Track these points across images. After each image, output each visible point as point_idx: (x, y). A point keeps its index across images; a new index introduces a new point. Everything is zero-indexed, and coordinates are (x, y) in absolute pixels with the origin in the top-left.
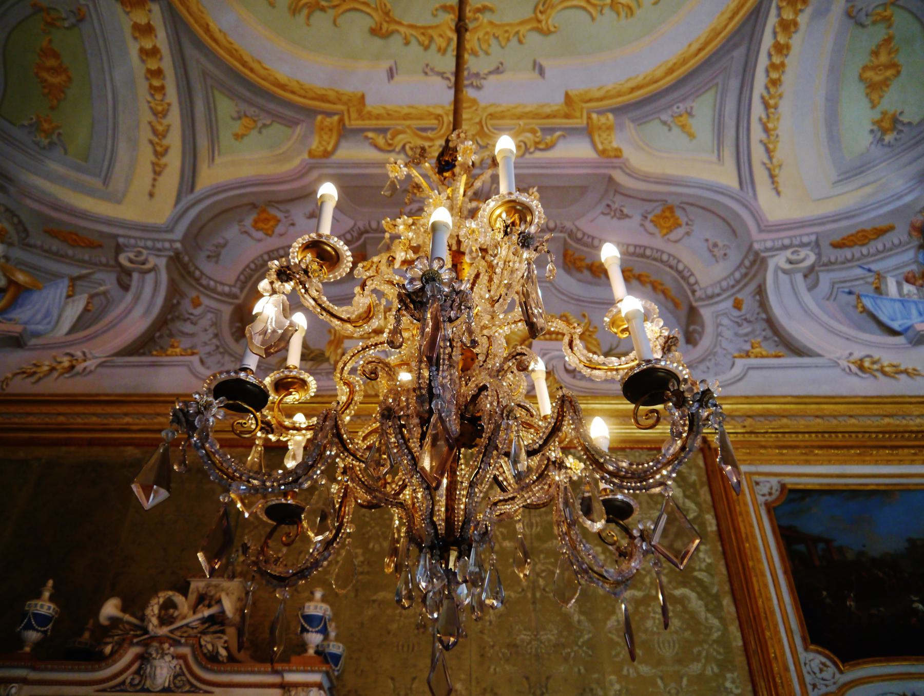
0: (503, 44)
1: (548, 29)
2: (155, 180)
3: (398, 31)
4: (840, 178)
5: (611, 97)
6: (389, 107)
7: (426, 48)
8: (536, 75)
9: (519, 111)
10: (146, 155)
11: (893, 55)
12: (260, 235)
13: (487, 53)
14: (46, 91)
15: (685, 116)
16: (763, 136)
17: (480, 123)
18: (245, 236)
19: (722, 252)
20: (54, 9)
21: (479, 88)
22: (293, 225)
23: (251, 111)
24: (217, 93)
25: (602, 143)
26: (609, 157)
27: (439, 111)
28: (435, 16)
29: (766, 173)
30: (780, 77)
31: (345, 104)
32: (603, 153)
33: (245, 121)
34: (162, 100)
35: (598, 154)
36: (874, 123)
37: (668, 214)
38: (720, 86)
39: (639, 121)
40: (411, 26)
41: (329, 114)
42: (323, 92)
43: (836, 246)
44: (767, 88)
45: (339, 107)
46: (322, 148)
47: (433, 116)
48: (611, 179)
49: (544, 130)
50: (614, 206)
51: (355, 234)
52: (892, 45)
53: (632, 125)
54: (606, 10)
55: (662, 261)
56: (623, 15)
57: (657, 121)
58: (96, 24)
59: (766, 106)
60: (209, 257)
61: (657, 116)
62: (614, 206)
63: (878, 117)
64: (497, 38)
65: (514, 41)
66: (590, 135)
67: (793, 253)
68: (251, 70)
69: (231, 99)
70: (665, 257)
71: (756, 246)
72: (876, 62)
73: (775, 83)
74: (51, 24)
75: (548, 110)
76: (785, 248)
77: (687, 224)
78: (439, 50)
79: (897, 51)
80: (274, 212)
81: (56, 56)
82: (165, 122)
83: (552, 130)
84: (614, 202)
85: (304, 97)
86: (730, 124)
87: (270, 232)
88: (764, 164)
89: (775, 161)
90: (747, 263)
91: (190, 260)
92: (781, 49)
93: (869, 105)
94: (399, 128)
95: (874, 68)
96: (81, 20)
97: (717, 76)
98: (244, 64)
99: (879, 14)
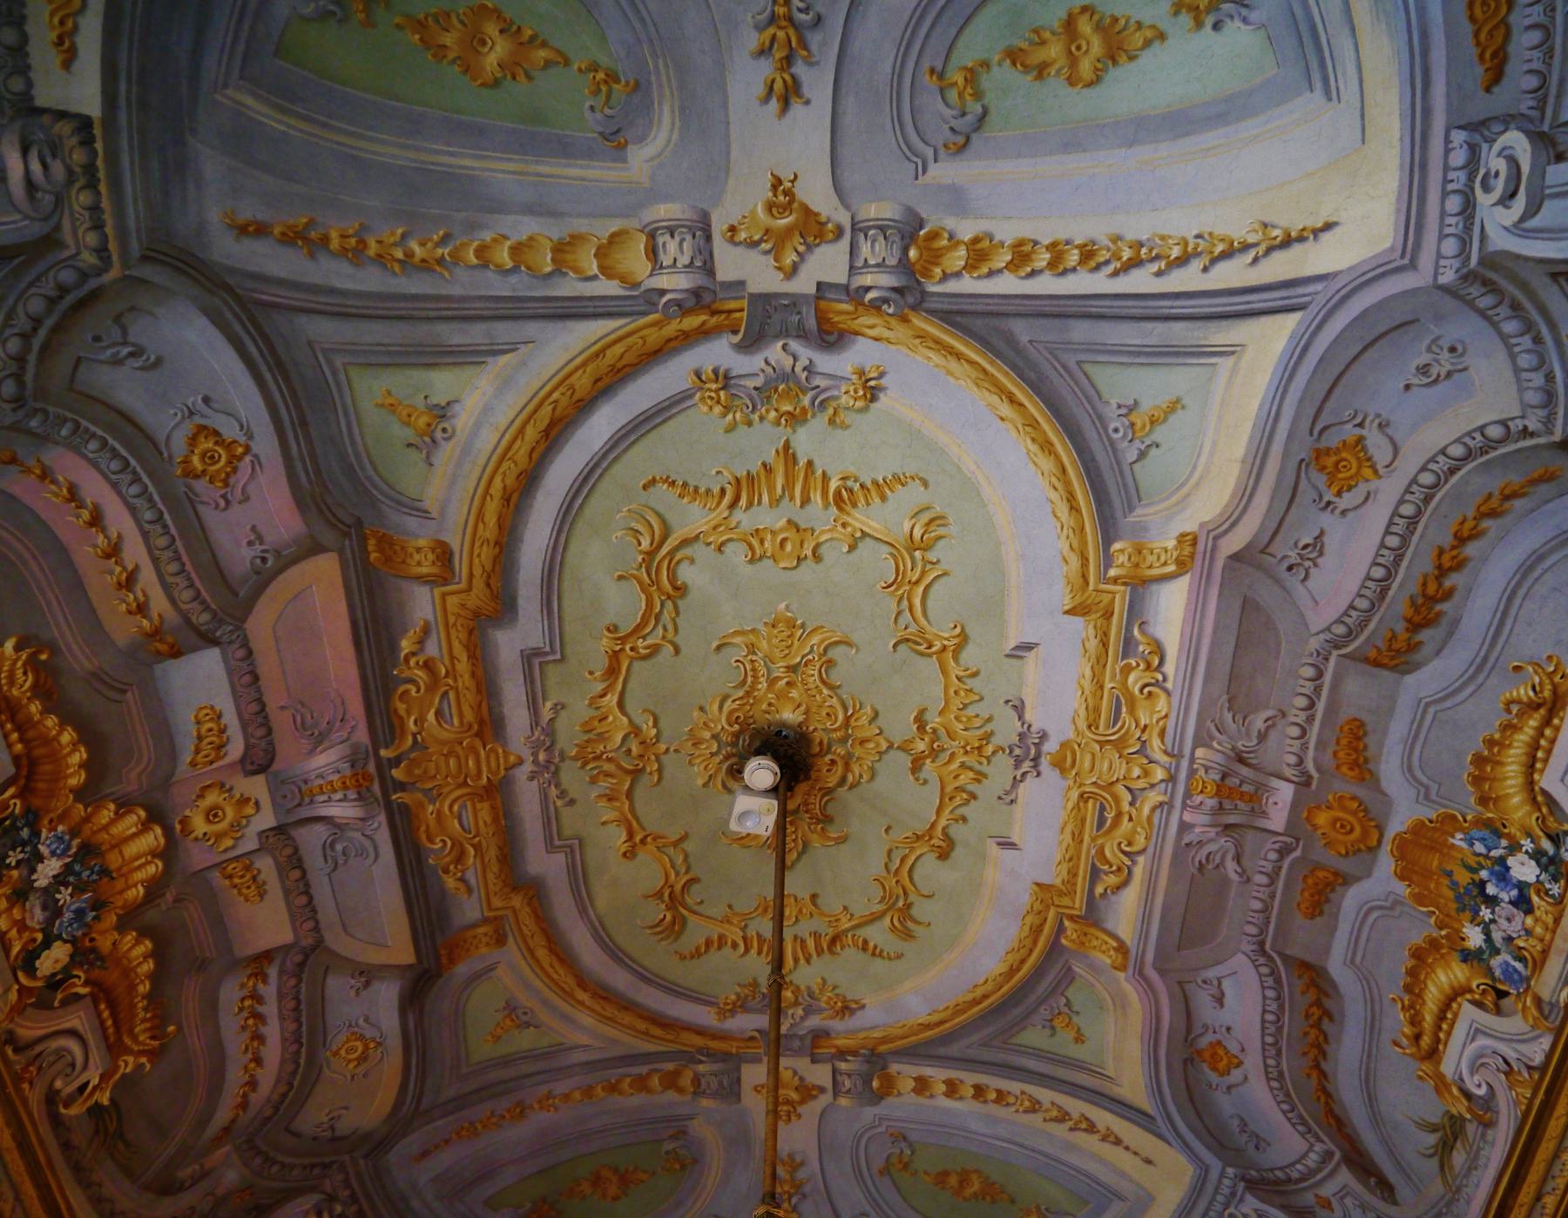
0: (977, 698)
1: (958, 636)
2: (1127, 1148)
3: (944, 829)
4: (1318, 85)
5: (1084, 543)
6: (1058, 857)
7: (973, 796)
8: (1031, 655)
9: (1087, 684)
10: (1090, 1142)
11: (1047, 35)
12: (1236, 1076)
13: (989, 720)
14: (988, 1198)
15: (1133, 418)
16: (1196, 265)
17: (1102, 744)
18: (1233, 1091)
19: (1446, 355)
20: (889, 1156)
21: (1044, 736)
22: (1228, 1029)
23: (1044, 1012)
24: (1014, 1040)
25: (1165, 564)
26: (1192, 556)
27: (1075, 794)
28: (925, 782)
29: (1279, 256)
30: (1077, 247)
31: (1048, 908)
32: (1183, 566)
33: (1056, 1022)
34: (1017, 1098)
35: (1187, 572)
36: (1199, 24)
37: (1330, 462)
38: (1082, 357)
39: (1134, 496)
40: (939, 812)
41: (1060, 930)
42: (1026, 928)
43: (1496, 75)
44: (1098, 268)
45: (1051, 913)
46: (1112, 953)
47: (1081, 804)
48: (1236, 557)
49: (1125, 655)
50: (1293, 557)
51: (1262, 960)
52: (1024, 45)
53: (1139, 511)
54: (932, 556)
55: (1436, 486)
56: (941, 531)
57: (1137, 467)
58: (913, 1126)
59: (1135, 263)
60: (1257, 1148)
61: (1127, 469)
62: (1293, 557)
63: (1186, 19)
64: (965, 706)
65: (971, 683)
66: (1146, 582)
67: (1487, 188)
68: (985, 997)
69: (1024, 1028)
70: (1427, 478)
71: (1447, 277)
72: (1062, 62)
73: (1087, 253)
74: (906, 1166)
75: (1093, 644)
76: (1468, 208)
77: (1361, 425)
78: (979, 781)
79: (1036, 31)
80: (1204, 1042)
81: (945, 1174)
82: (1047, 1105)
83: (1128, 645)
84: (1285, 557)
85: (1031, 951)
86: (1157, 333)
87: (1236, 1061)
88: (1256, 260)
89: (1251, 239)
90: (1485, 302)
91: (1258, 1171)
92: (1021, 255)
93: (1157, 44)
94: (1093, 852)
95: (1073, 62)
96: (905, 1139)
97: (1064, 366)
98: (976, 1002)
99: (961, 95)
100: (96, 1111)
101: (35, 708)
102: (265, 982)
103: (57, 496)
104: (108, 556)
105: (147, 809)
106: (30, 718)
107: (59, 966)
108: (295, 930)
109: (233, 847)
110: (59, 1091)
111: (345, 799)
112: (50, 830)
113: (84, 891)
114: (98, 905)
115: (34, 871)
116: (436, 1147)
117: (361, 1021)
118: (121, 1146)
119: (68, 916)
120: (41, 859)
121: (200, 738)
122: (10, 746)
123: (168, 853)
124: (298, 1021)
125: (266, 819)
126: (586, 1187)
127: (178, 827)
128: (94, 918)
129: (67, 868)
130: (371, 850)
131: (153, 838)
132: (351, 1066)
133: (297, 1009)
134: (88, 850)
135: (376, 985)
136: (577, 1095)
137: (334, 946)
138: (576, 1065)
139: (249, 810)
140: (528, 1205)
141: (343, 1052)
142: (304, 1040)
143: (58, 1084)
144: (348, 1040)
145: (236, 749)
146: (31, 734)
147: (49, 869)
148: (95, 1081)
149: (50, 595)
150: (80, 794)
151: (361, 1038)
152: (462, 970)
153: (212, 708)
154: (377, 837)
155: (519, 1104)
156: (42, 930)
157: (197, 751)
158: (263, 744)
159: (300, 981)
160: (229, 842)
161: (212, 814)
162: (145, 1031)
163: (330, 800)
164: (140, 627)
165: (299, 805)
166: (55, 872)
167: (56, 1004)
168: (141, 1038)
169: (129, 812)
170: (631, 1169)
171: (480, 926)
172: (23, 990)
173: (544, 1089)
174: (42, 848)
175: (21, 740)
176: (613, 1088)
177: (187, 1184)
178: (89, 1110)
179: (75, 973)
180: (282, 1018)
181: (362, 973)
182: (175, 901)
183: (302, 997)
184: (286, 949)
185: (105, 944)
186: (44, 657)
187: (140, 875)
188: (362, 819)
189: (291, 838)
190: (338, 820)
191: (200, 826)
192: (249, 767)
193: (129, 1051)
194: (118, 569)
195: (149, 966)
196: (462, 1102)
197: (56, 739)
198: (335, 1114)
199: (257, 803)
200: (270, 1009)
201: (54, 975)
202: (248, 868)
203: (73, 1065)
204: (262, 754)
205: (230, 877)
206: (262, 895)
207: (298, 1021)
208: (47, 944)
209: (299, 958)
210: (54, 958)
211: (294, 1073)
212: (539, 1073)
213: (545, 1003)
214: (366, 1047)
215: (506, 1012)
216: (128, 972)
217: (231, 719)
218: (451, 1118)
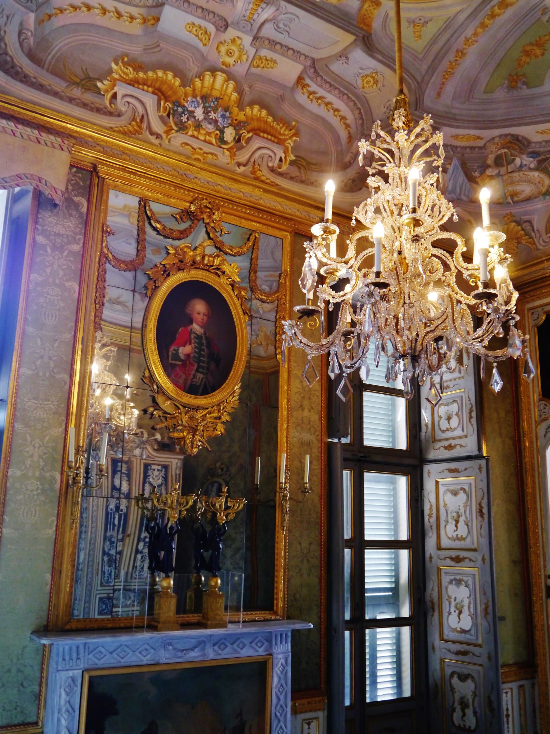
100: (292, 163)
101: (141, 75)
102: (309, 86)
103: (71, 13)
104: (105, 13)
105: (208, 71)
106: (144, 79)
107: (234, 135)
108: (300, 63)
109: (248, 57)
110: (273, 167)
111: (263, 9)
112: (187, 102)
113: (217, 109)
114: (226, 109)
115: (195, 117)
116: (441, 88)
117: (360, 71)
118: (312, 166)
119: (220, 120)
120: (194, 112)
121: (197, 36)
122: (147, 91)
123: (230, 77)
124: (336, 88)
125: (247, 40)
126: (524, 59)
127: (224, 67)
128: (230, 114)
129: (204, 107)
130: (294, 17)
131: (220, 77)
132: (375, 87)
133: (331, 85)
134: (205, 98)
135: (350, 56)
136: (479, 30)
137: (319, 57)
138: (466, 19)
139: (238, 42)
140: (506, 81)
141: (365, 85)
142: (346, 92)
143: (270, 164)
144: (363, 80)
145: (211, 29)
146: (149, 83)
147: (199, 113)
148: (283, 156)
149: (105, 41)
150: (184, 84)
151: (367, 76)
152: (376, 25)
153: (188, 24)
154: (289, 10)
155: (457, 51)
156: (217, 130)
157: (201, 40)
158: (217, 18)
159: (321, 77)
160: (244, 57)
161: (229, 53)
162: (285, 130)
163: (259, 14)
164: (139, 23)
165: (252, 25)
166: (202, 112)
167: (245, 145)
168: (286, 133)
169: (204, 76)
170: (538, 39)
171: (363, 6)
172: (228, 150)
173: (462, 39)
174: (191, 109)
175: (148, 87)
176: (493, 16)
177: (352, 161)
178: (290, 164)
179: (241, 132)
180: (330, 92)
181: (340, 57)
182: (250, 87)
183: (328, 80)
184: (304, 71)
185: (241, 117)
186: (126, 59)
187: (230, 90)
188: (277, 10)
189: (262, 38)
190: (270, 18)
191: (230, 60)
192: (222, 29)
193: (287, 139)
194: (112, 14)
195: (264, 113)
196: (432, 68)
197: (157, 77)
198: (387, 105)
199: (238, 38)
200: (321, 92)
201: (235, 138)
202: (260, 59)
203: (270, 156)
204: (220, 22)
205: (258, 66)
206: (275, 62)
207: (336, 88)
208: (222, 132)
209: (312, 70)
210: (229, 134)
211: (355, 103)
212: (452, 36)
213: (422, 9)
214: (373, 78)
215: (412, 25)
216: (259, 119)
217: (198, 21)
218: (435, 75)
